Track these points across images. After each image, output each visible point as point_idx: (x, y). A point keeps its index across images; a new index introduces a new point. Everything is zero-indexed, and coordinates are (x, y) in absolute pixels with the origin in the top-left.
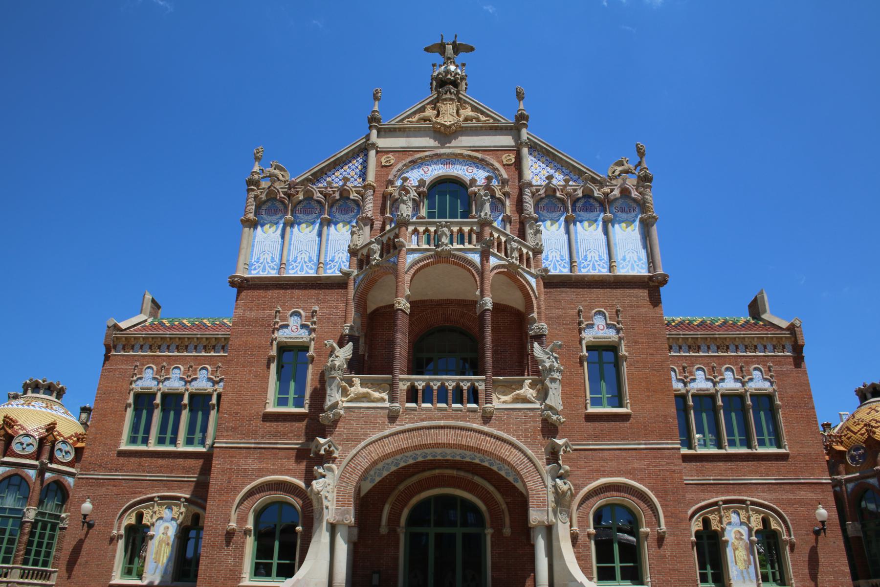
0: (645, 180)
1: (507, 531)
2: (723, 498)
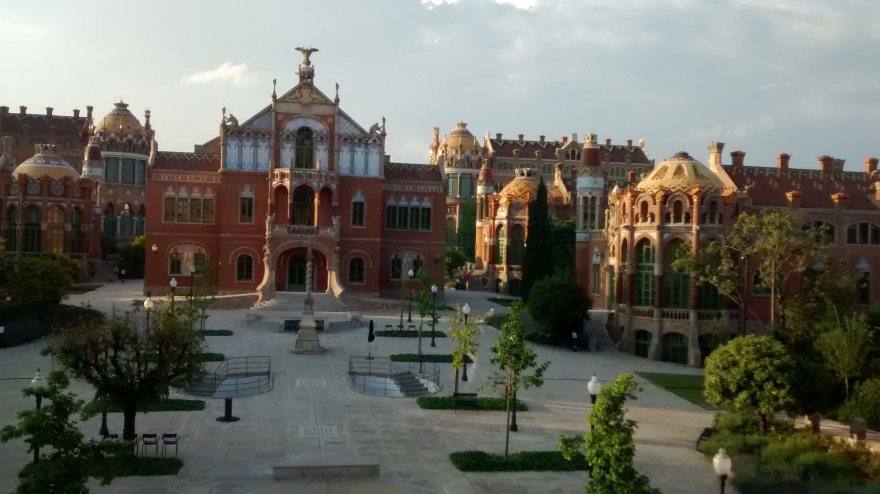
0: (384, 135)
1: (322, 265)
2: (404, 248)
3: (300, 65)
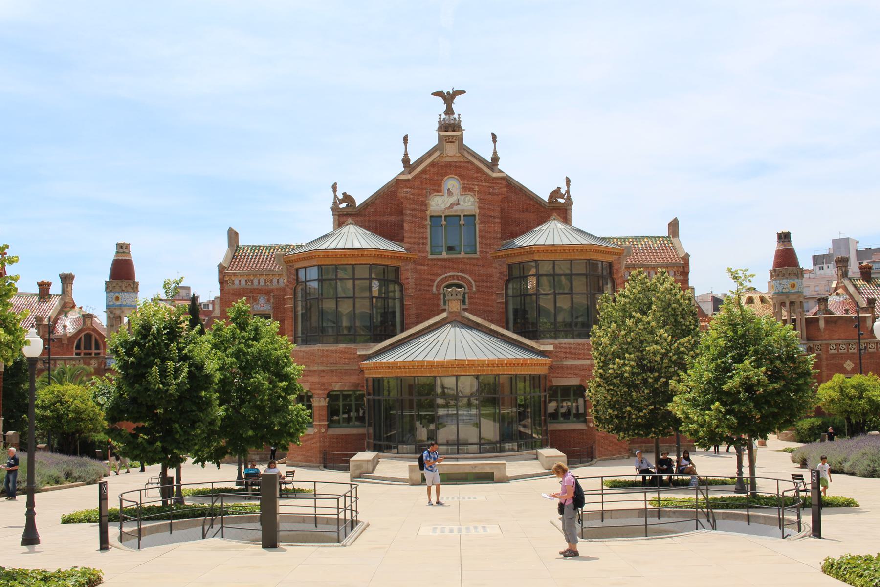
0: (569, 202)
3: (440, 115)
